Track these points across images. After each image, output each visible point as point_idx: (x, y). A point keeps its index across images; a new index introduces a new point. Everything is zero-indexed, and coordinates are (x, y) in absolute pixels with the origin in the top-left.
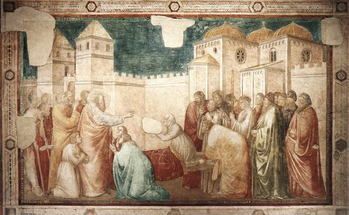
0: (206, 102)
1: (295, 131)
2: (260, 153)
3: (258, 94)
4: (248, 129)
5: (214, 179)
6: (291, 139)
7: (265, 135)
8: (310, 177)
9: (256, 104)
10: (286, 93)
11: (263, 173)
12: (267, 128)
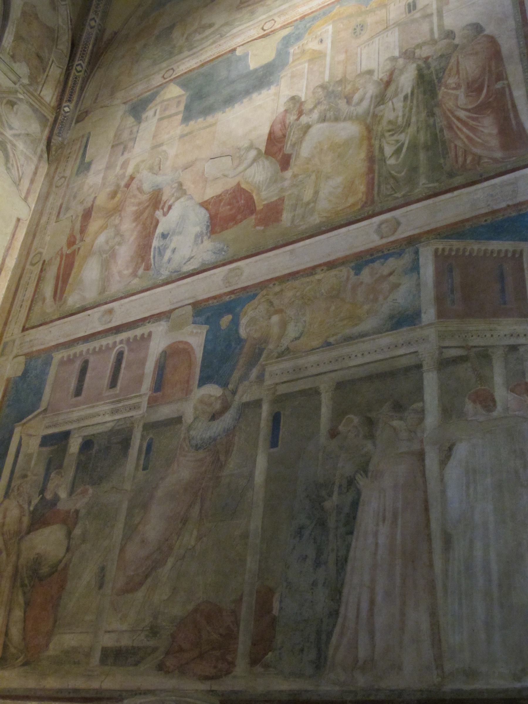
0: (302, 104)
1: (457, 77)
2: (391, 133)
3: (386, 60)
6: (451, 91)
7: (399, 103)
8: (495, 131)
9: (383, 73)
10: (436, 36)
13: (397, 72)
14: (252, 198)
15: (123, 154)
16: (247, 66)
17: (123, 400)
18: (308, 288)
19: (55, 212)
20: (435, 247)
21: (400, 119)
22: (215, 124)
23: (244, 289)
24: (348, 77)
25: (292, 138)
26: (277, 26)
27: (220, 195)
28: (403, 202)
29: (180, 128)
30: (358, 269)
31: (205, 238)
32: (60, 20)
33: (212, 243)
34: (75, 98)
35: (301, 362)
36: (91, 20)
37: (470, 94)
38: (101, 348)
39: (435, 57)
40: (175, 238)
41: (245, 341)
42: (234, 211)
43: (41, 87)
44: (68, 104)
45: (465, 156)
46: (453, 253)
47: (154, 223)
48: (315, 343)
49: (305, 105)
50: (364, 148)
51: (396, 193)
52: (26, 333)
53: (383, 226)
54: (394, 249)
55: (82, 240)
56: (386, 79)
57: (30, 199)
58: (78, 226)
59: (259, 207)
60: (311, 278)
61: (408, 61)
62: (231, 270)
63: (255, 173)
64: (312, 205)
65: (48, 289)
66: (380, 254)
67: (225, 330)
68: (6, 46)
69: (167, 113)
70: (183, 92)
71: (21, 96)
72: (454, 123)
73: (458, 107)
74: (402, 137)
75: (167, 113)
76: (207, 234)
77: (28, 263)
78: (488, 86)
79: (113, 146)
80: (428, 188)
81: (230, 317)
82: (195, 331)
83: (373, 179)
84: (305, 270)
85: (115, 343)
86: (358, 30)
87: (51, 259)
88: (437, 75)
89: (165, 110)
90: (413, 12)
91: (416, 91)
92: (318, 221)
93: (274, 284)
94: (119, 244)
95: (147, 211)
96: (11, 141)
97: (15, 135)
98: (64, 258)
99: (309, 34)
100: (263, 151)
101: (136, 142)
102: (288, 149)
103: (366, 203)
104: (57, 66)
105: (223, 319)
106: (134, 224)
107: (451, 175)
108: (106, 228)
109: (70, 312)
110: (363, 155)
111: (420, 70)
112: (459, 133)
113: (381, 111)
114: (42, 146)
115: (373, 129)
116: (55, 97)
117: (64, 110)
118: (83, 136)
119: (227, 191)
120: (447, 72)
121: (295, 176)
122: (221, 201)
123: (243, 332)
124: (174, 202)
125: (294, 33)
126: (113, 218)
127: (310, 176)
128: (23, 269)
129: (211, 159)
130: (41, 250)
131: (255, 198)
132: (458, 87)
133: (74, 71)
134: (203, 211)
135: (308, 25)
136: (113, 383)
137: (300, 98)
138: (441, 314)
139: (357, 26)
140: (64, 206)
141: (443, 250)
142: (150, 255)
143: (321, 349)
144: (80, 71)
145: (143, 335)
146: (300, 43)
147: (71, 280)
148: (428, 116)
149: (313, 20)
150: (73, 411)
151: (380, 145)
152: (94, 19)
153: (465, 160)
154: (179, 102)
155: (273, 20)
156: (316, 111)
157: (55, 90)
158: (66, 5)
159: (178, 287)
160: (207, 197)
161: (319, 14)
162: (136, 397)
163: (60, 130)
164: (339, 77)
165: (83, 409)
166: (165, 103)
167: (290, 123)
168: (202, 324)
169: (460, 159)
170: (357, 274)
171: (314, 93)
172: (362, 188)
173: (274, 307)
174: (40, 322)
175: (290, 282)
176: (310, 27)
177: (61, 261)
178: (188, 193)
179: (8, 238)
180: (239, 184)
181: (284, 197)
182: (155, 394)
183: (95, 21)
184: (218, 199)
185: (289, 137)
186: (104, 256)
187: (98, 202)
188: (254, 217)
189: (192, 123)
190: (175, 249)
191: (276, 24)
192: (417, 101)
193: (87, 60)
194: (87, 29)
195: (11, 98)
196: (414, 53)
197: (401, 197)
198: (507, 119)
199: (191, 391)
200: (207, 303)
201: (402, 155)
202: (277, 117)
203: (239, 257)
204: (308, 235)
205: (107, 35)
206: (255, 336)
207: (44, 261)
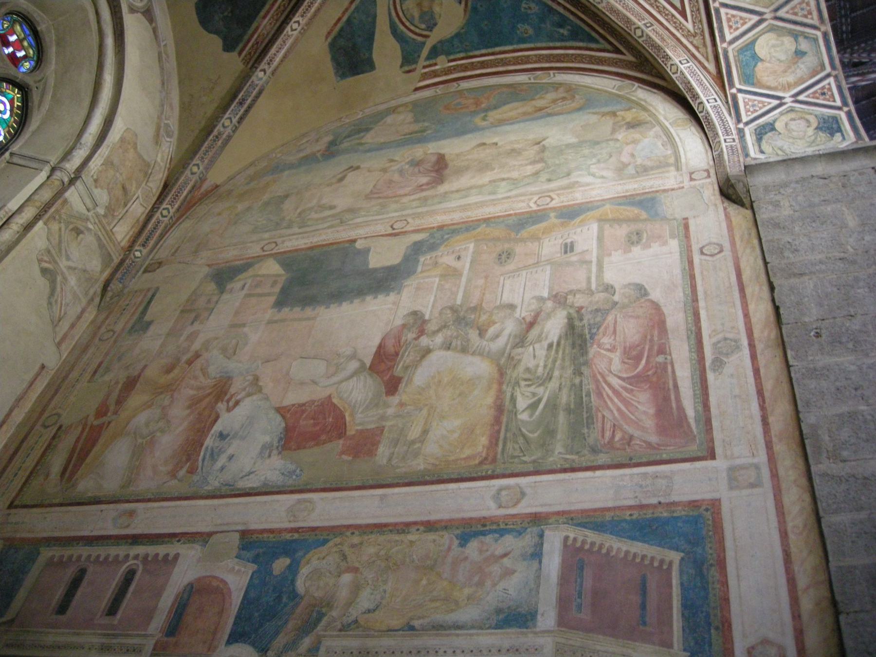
0: (425, 322)
1: (613, 338)
3: (533, 298)
4: (505, 348)
5: (412, 438)
7: (541, 352)
8: (652, 411)
11: (531, 416)
12: (549, 341)
13: (543, 314)
14: (344, 417)
15: (192, 323)
16: (366, 263)
17: (121, 635)
18: (396, 548)
19: (90, 370)
20: (564, 534)
21: (540, 370)
22: (314, 318)
23: (313, 529)
24: (484, 305)
25: (407, 358)
26: (409, 228)
27: (304, 405)
28: (532, 469)
29: (270, 311)
30: (464, 540)
31: (275, 452)
32: (160, 155)
33: (282, 462)
34: (152, 243)
35: (370, 643)
36: (194, 165)
37: (626, 361)
38: (106, 558)
39: (589, 309)
40: (235, 443)
41: (302, 598)
42: (318, 428)
43: (116, 221)
44: (142, 248)
45: (614, 431)
46: (587, 547)
47: (213, 417)
48: (396, 623)
49: (429, 325)
50: (493, 393)
51: (524, 456)
52: (13, 511)
53: (504, 493)
54: (513, 524)
55: (116, 413)
56: (528, 319)
57: (63, 346)
58: (114, 396)
59: (350, 432)
60: (402, 537)
61: (558, 306)
62: (299, 501)
63: (352, 389)
64: (417, 445)
65: (57, 462)
66: (494, 527)
67: (277, 576)
68: (92, 168)
69: (259, 290)
70: (283, 272)
71: (91, 226)
72: (604, 389)
73: (610, 372)
74: (541, 390)
75: (259, 290)
76: (277, 447)
77: (40, 423)
78: (648, 357)
79: (182, 312)
80: (566, 460)
81: (288, 561)
82: (237, 568)
83: (499, 432)
84: (396, 524)
85: (127, 556)
86: (504, 257)
87: (71, 426)
88: (590, 329)
89: (257, 286)
90: (569, 254)
91: (563, 342)
92: (422, 467)
93: (353, 533)
94: (163, 431)
95: (207, 400)
96: (63, 274)
97: (70, 268)
98: (87, 430)
99: (446, 246)
100: (368, 365)
101: (213, 314)
102: (398, 371)
103: (486, 459)
104: (141, 204)
105: (277, 561)
106: (188, 411)
107: (594, 450)
108: (150, 407)
109: (78, 501)
110: (490, 400)
111: (570, 319)
112: (609, 403)
113: (519, 355)
114: (98, 287)
115: (506, 372)
116: (128, 237)
117: (134, 255)
118: (149, 290)
119: (313, 402)
120: (601, 330)
121: (402, 405)
122: (303, 412)
123: (300, 585)
124: (244, 398)
125: (428, 241)
126: (162, 396)
127: (421, 410)
128: (32, 428)
129: (302, 358)
130: (60, 411)
131: (348, 419)
132: (612, 349)
133: (158, 215)
134: (279, 418)
135: (446, 237)
136: (112, 611)
137: (423, 315)
138: (563, 621)
139: (503, 253)
140: (104, 365)
141: (575, 539)
142: (199, 456)
143: (401, 632)
144: (166, 217)
145: (167, 555)
146: (434, 254)
147: (88, 460)
148: (574, 374)
149: (452, 233)
150: (49, 633)
151: (512, 395)
152: (198, 165)
153: (613, 436)
154: (275, 283)
155: (406, 220)
156: (440, 335)
157: (132, 228)
158: (171, 142)
159: (228, 505)
160: (287, 402)
161: (461, 228)
162: (138, 635)
163: (123, 275)
164: (474, 302)
165: (63, 634)
166: (258, 278)
167: (406, 340)
168: (249, 561)
169: (608, 434)
170: (462, 545)
171: (441, 313)
172: (484, 440)
173: (347, 562)
174: (35, 502)
175: (373, 536)
176: (448, 239)
177: (82, 432)
178: (265, 391)
179: (24, 386)
180: (330, 397)
181: (384, 427)
182: (166, 639)
183: (199, 169)
184: (300, 409)
185: (403, 356)
186: (140, 441)
187: (148, 373)
188: (341, 442)
189: (286, 310)
190: (233, 456)
191: (408, 226)
192: (563, 353)
193: (176, 206)
194: (188, 172)
195: (80, 225)
196: (566, 299)
197: (530, 463)
198: (667, 399)
199: (216, 648)
200: (260, 536)
201: (537, 413)
202: (391, 330)
203: (314, 487)
204: (406, 481)
205: (206, 186)
206: (316, 595)
207: (61, 427)
